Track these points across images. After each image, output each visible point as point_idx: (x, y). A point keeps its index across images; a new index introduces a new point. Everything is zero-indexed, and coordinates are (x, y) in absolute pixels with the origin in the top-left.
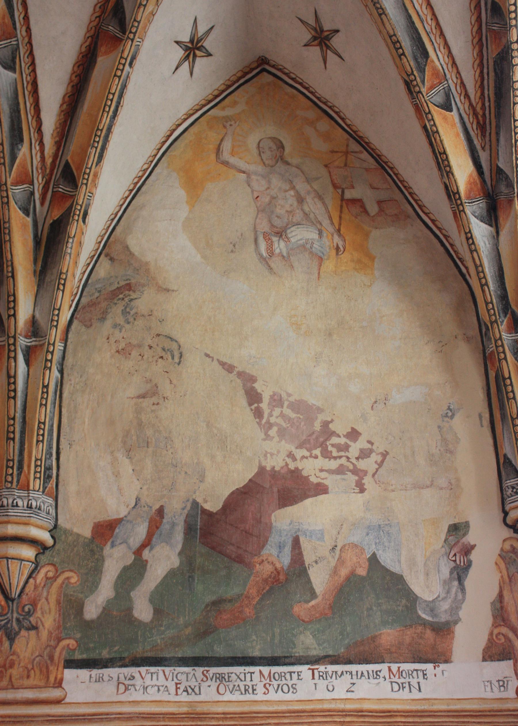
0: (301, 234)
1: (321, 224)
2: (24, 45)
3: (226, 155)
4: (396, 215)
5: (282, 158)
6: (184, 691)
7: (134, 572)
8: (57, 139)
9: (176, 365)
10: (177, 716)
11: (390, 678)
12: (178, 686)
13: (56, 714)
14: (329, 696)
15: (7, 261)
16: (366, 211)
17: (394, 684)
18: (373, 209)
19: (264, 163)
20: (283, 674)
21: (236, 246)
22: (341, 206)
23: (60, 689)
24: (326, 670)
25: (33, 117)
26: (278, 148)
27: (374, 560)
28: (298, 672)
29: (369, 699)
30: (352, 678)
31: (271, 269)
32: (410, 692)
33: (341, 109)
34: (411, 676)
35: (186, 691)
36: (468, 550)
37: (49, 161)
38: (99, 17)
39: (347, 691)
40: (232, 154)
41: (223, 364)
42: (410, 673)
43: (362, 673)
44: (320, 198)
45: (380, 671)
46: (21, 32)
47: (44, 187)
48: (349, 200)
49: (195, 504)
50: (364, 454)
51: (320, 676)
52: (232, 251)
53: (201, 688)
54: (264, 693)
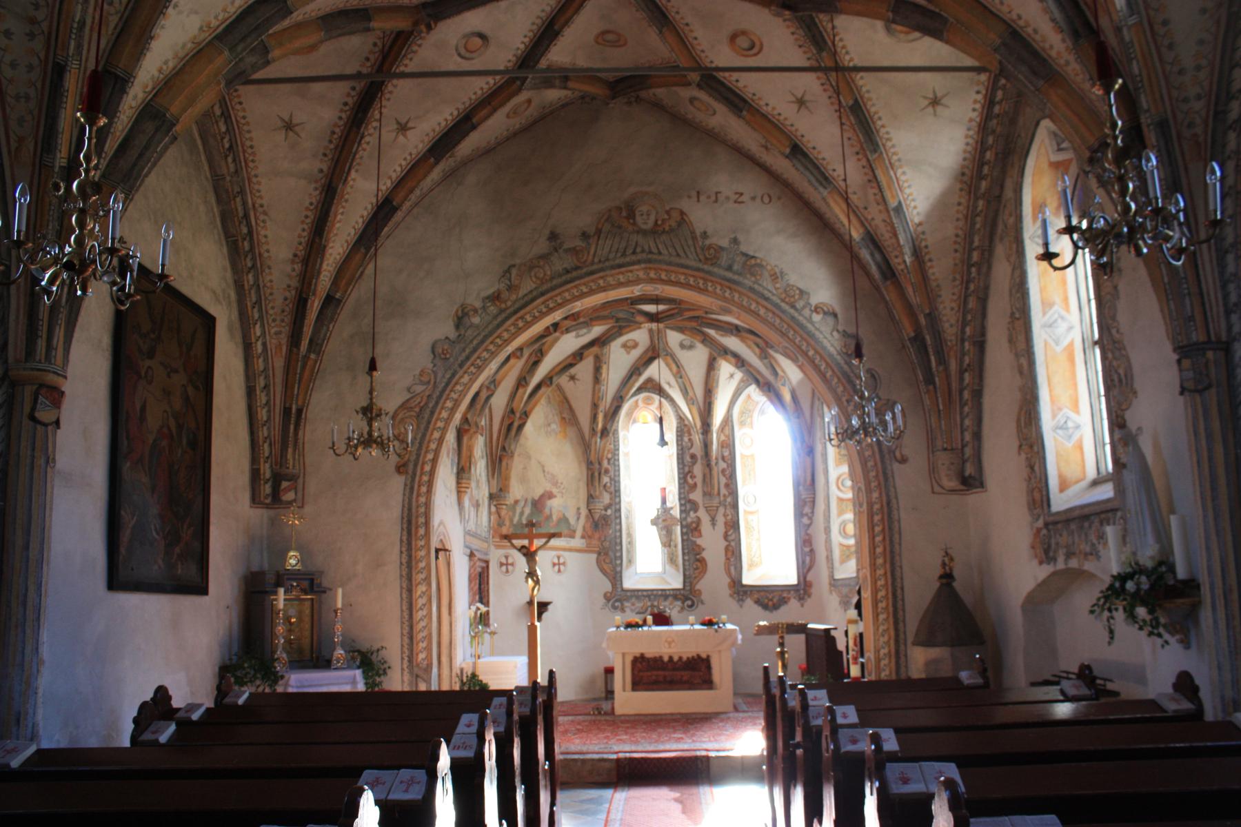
0: (554, 426)
7: (522, 513)
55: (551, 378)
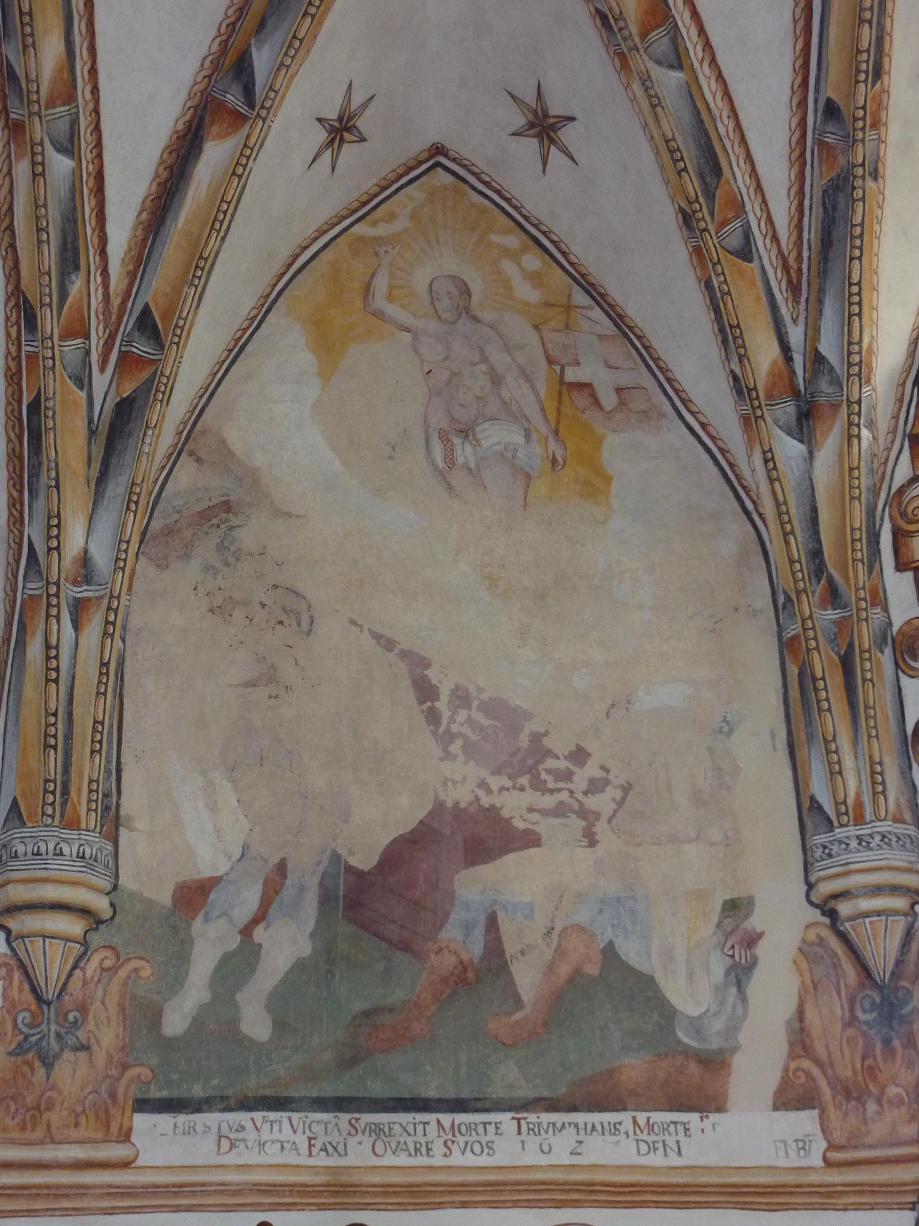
0: (497, 435)
1: (528, 420)
2: (88, 114)
3: (379, 302)
4: (645, 412)
5: (467, 310)
6: (321, 1150)
7: (241, 961)
8: (131, 267)
9: (305, 636)
10: (312, 1189)
11: (635, 1134)
12: (313, 1142)
13: (122, 1183)
14: (543, 1160)
15: (49, 461)
16: (597, 402)
17: (641, 1143)
18: (609, 400)
19: (439, 317)
20: (473, 1126)
21: (397, 449)
22: (560, 394)
23: (128, 1144)
24: (539, 1121)
25: (94, 230)
26: (461, 295)
27: (610, 951)
28: (496, 1124)
29: (604, 1166)
30: (578, 1134)
31: (451, 488)
32: (666, 1155)
33: (563, 237)
34: (666, 1132)
35: (325, 1150)
36: (751, 940)
37: (116, 302)
38: (209, 77)
39: (571, 1153)
40: (390, 298)
41: (377, 637)
42: (666, 1126)
43: (593, 1126)
44: (528, 379)
45: (620, 1124)
46: (83, 92)
47: (106, 343)
48: (571, 384)
49: (336, 858)
50: (596, 787)
51: (529, 1129)
52: (390, 457)
53: (348, 1146)
54: (445, 1155)
55: (242, 69)
